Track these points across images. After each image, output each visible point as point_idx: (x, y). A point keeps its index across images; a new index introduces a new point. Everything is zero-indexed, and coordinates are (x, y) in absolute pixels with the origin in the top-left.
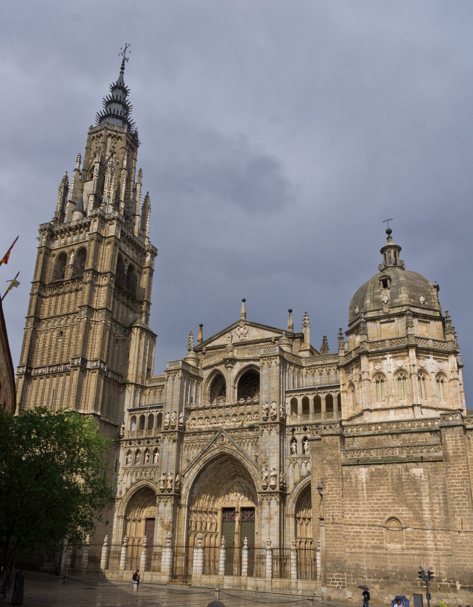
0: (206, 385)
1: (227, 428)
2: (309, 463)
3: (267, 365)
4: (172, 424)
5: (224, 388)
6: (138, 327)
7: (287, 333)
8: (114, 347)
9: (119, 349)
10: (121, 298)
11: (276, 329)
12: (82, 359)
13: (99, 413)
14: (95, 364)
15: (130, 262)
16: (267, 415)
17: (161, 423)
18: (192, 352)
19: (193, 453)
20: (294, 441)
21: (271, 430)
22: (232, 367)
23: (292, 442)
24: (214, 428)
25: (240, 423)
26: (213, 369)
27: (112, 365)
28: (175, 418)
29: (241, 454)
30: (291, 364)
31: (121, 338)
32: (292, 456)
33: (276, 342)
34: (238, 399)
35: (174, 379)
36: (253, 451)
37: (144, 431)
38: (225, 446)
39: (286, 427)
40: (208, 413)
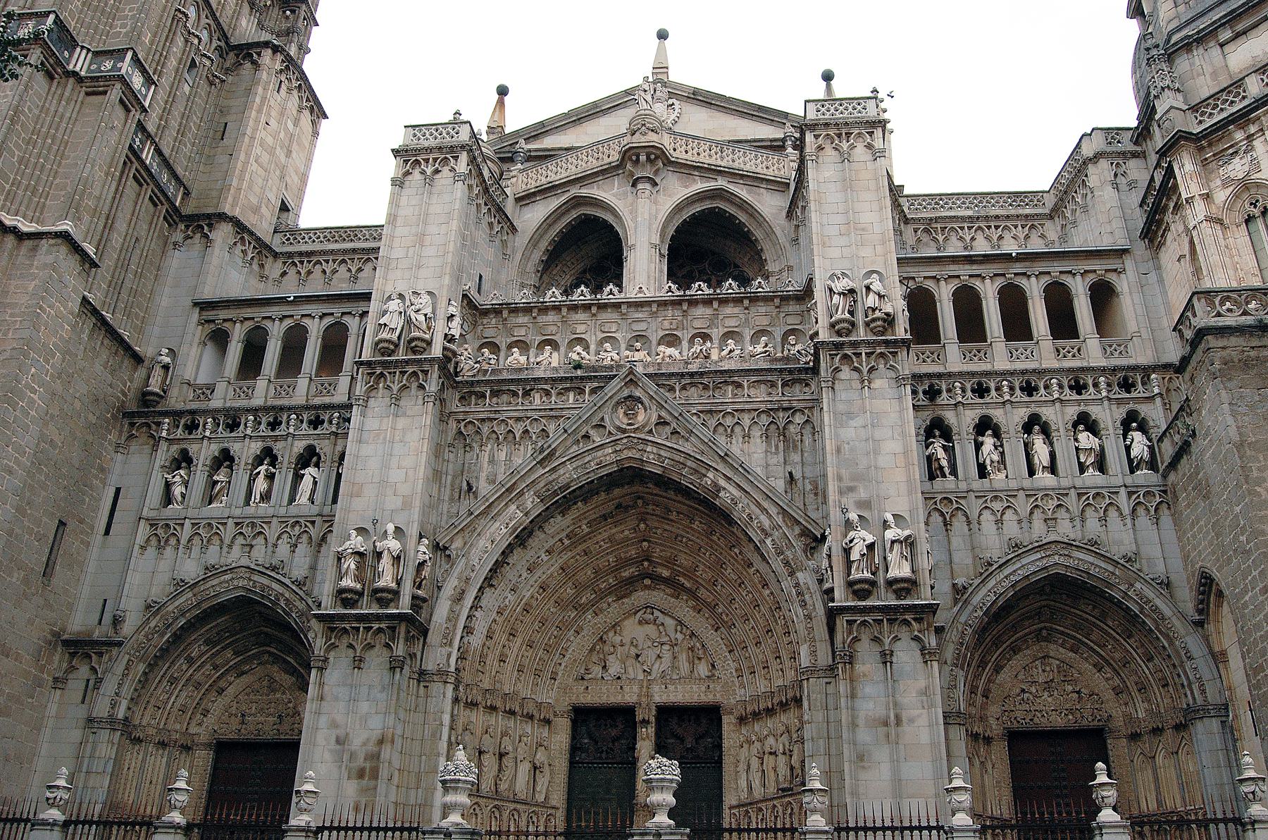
0: (526, 257)
1: (651, 370)
2: (1009, 513)
3: (834, 153)
4: (417, 334)
6: (276, 49)
8: (178, 80)
12: (55, 22)
14: (108, 65)
16: (851, 313)
19: (492, 461)
20: (937, 433)
21: (871, 370)
23: (929, 433)
26: (563, 199)
28: (428, 310)
29: (721, 467)
31: (208, 63)
32: (939, 483)
35: (429, 181)
37: (261, 384)
38: (642, 436)
40: (554, 329)
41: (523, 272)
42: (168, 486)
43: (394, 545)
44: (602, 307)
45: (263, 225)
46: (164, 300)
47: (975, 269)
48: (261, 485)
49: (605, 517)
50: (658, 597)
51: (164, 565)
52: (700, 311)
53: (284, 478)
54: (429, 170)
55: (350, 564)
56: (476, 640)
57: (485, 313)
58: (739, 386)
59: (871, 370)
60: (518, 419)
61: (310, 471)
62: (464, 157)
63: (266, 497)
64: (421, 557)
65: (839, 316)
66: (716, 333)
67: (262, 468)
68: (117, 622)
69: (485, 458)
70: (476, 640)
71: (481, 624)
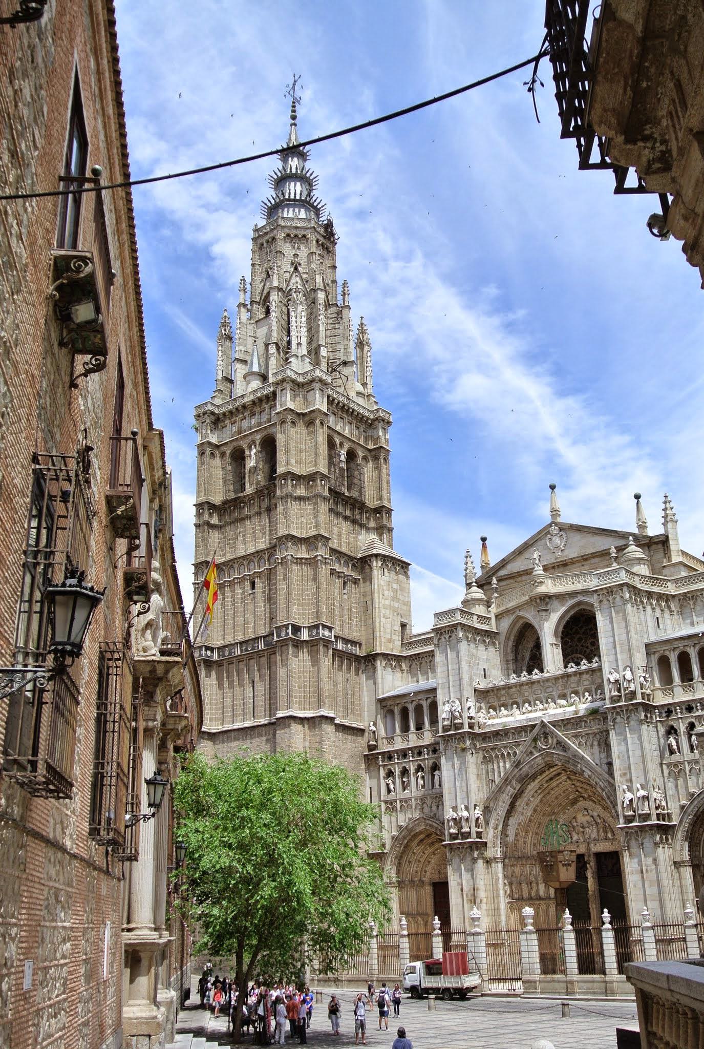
5: (538, 646)
6: (377, 556)
7: (636, 538)
8: (341, 595)
9: (349, 597)
10: (340, 509)
11: (616, 532)
13: (332, 715)
14: (314, 632)
15: (347, 446)
17: (437, 721)
18: (475, 589)
21: (628, 718)
22: (547, 610)
24: (529, 720)
25: (573, 708)
27: (341, 626)
28: (459, 709)
30: (650, 595)
33: (620, 554)
34: (566, 667)
36: (604, 755)
39: (655, 707)
41: (506, 654)
42: (388, 785)
43: (465, 814)
44: (533, 683)
45: (396, 649)
46: (366, 699)
47: (686, 642)
48: (421, 782)
49: (551, 779)
50: (588, 804)
51: (393, 819)
52: (573, 679)
53: (428, 777)
54: (447, 637)
55: (452, 823)
56: (511, 838)
57: (488, 691)
58: (586, 722)
59: (628, 718)
60: (505, 748)
61: (437, 773)
62: (459, 628)
63: (423, 787)
64: (477, 816)
65: (613, 694)
66: (581, 689)
67: (419, 774)
68: (383, 845)
69: (495, 765)
70: (511, 838)
71: (511, 831)
